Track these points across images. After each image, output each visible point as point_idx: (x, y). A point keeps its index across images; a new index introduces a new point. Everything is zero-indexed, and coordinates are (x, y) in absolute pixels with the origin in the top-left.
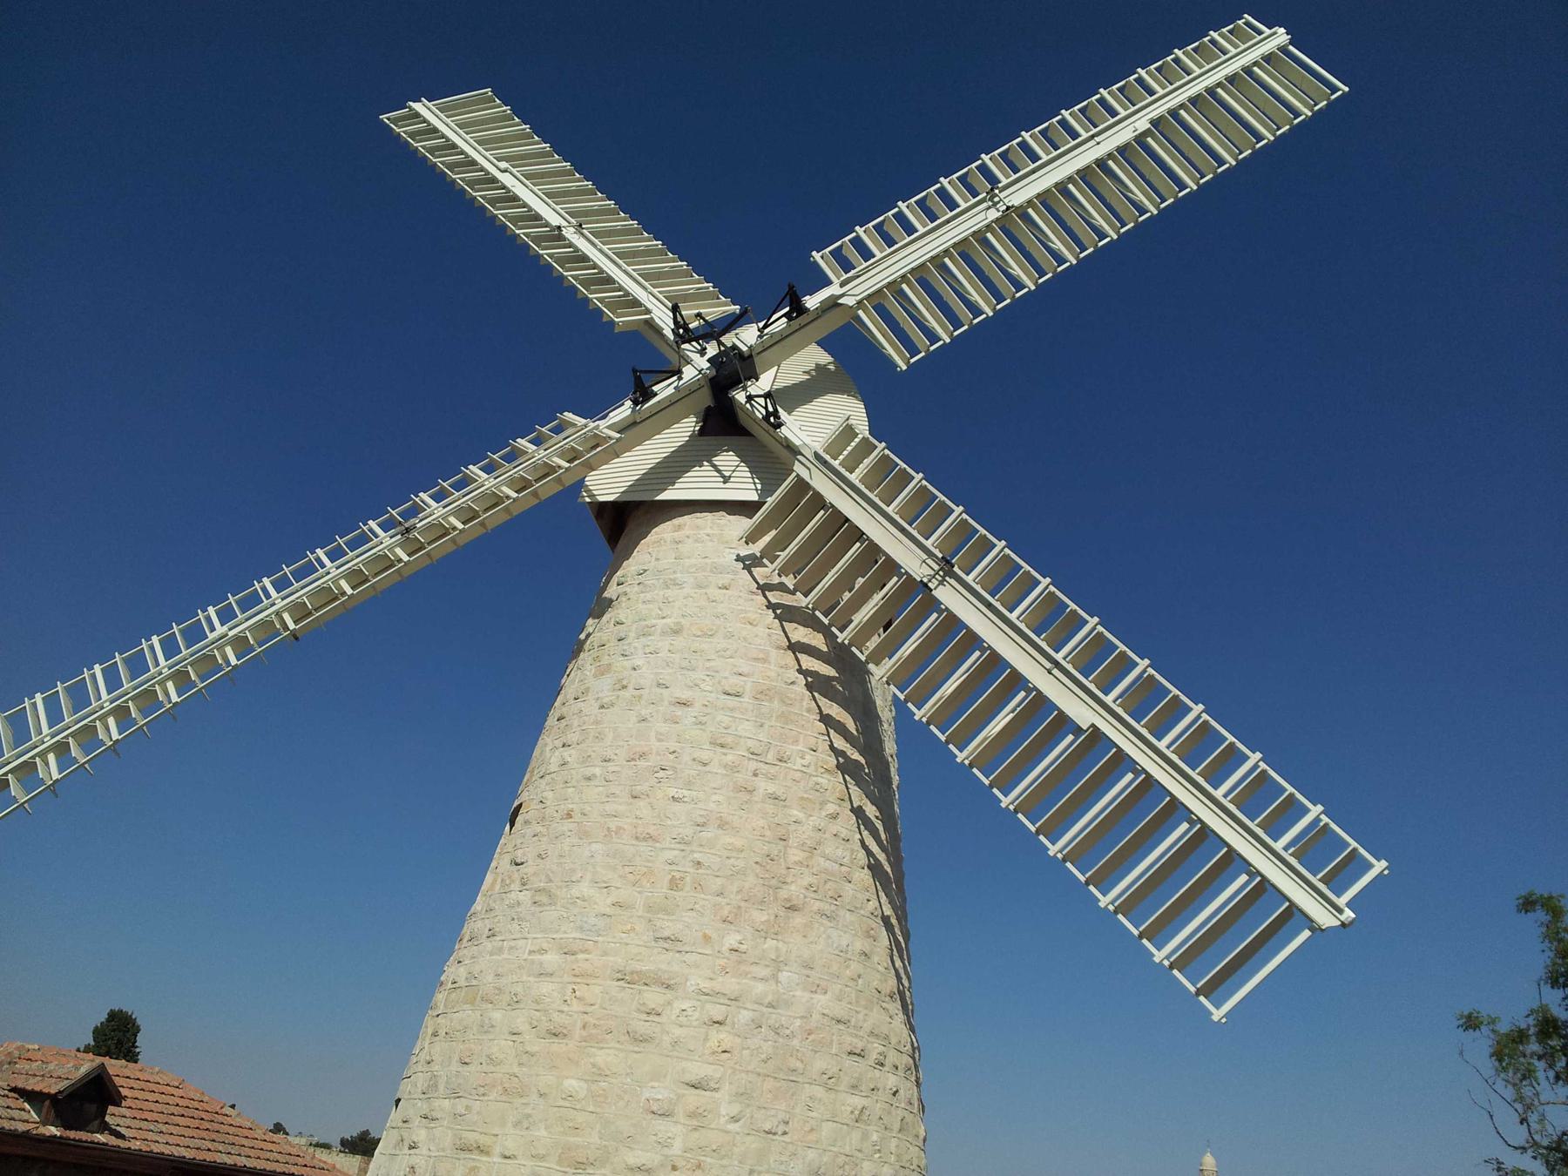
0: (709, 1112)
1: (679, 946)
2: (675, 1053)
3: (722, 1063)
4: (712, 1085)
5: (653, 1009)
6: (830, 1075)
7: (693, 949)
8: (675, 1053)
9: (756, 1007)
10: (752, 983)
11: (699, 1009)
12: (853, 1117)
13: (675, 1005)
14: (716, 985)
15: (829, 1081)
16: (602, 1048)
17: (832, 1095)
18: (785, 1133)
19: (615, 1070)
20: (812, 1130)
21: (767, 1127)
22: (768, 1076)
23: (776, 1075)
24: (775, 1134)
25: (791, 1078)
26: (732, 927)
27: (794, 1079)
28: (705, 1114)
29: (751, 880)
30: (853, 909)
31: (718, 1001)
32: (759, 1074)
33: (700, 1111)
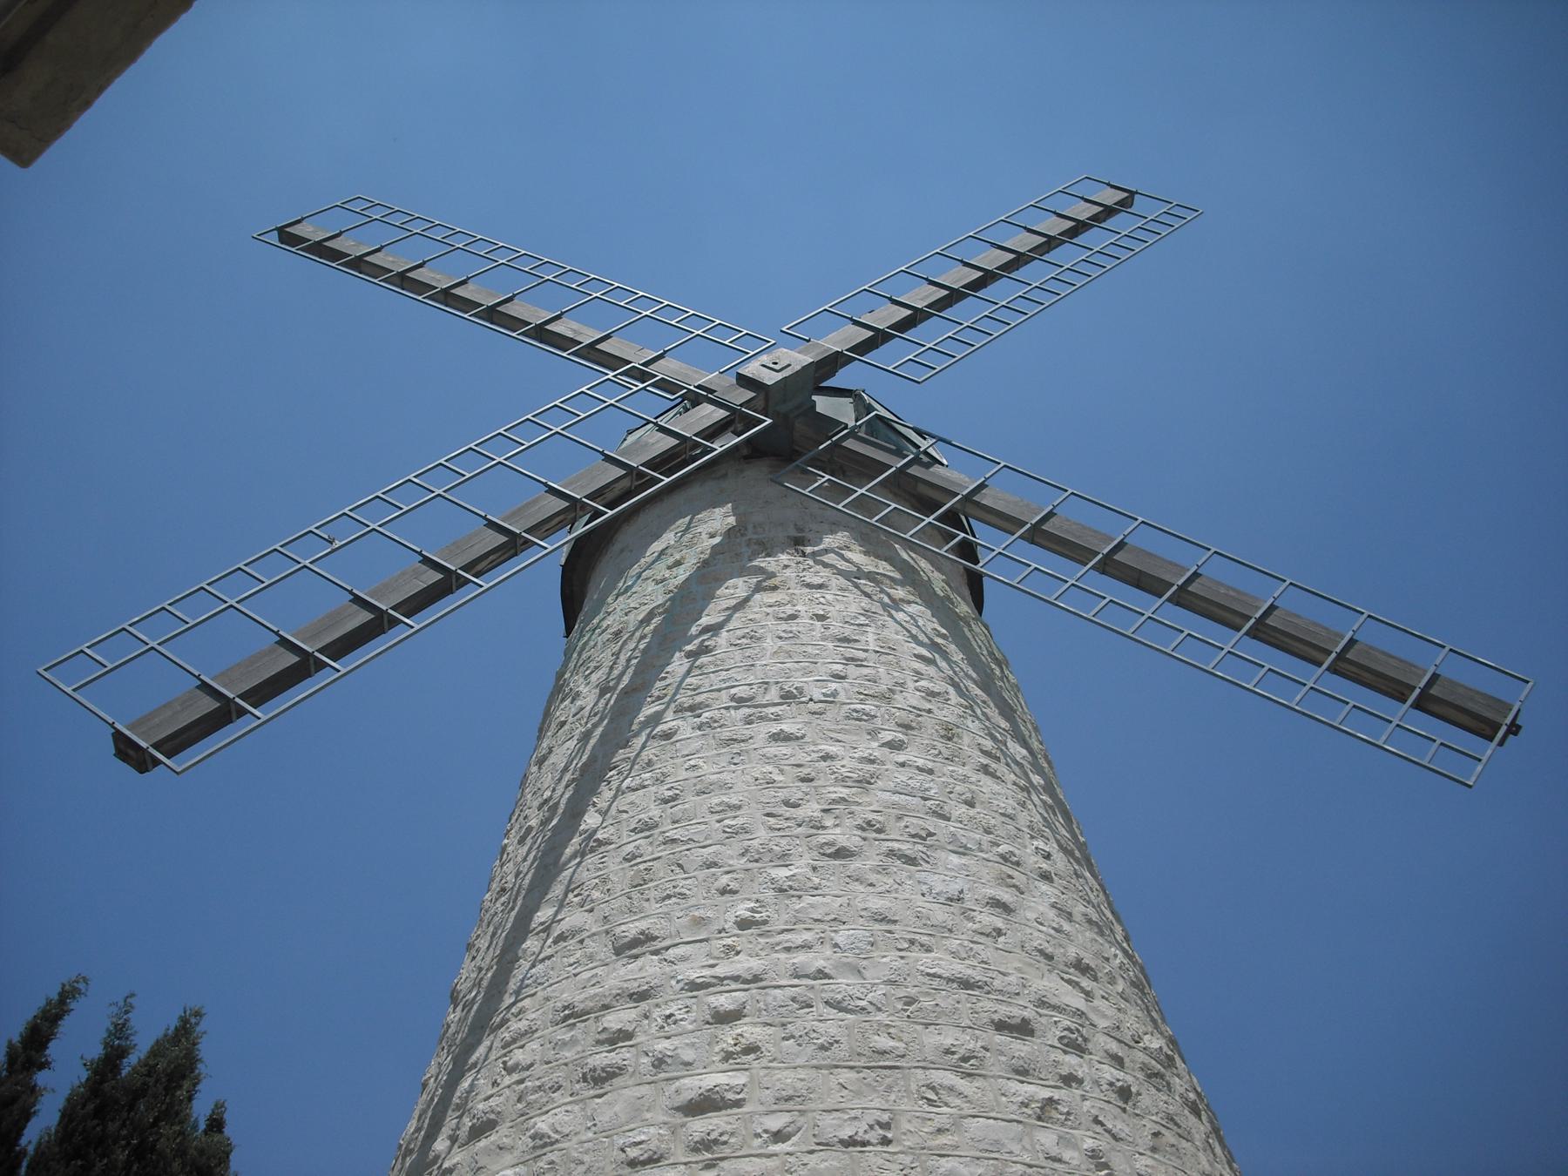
0: (732, 1134)
1: (658, 945)
2: (663, 1075)
3: (746, 1066)
4: (730, 1096)
5: (620, 1030)
6: (962, 1051)
7: (678, 940)
8: (663, 1075)
9: (796, 982)
10: (783, 956)
11: (695, 1007)
12: (1029, 1111)
13: (656, 1013)
14: (720, 971)
15: (967, 1065)
16: (547, 1112)
17: (979, 1082)
18: (886, 1141)
19: (566, 1131)
20: (940, 1131)
21: (846, 1133)
22: (837, 1067)
23: (852, 1064)
24: (864, 1144)
25: (881, 1064)
26: (736, 897)
27: (887, 1063)
28: (724, 1138)
29: (762, 834)
30: (961, 850)
31: (727, 988)
32: (817, 1067)
33: (712, 1137)
